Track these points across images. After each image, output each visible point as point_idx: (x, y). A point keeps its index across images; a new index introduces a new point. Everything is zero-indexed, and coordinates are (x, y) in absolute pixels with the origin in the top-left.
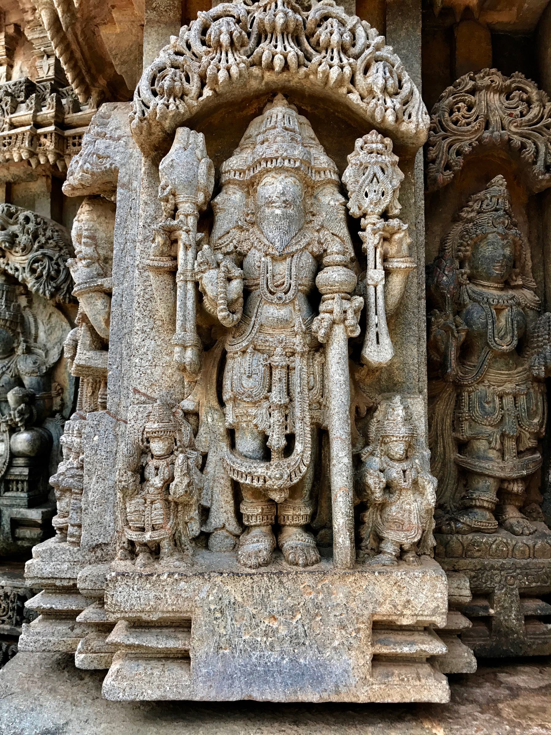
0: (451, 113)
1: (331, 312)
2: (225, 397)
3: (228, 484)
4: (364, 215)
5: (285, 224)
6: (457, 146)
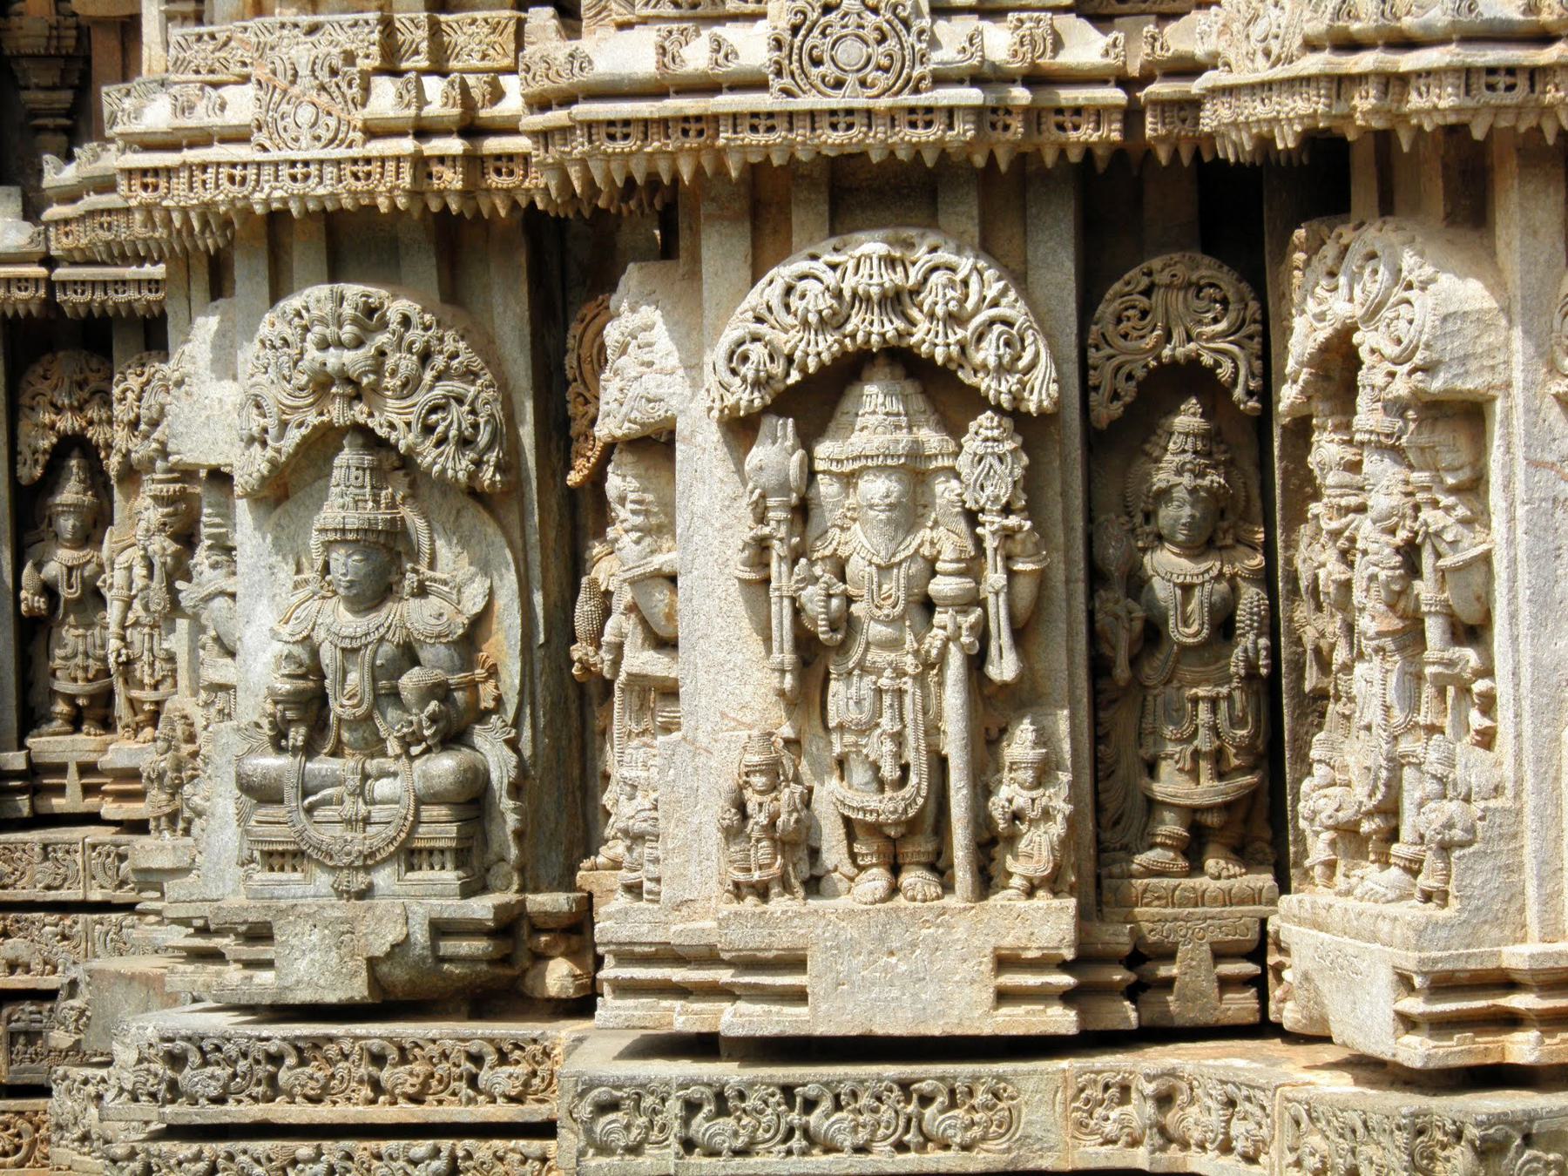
0: (1119, 321)
1: (944, 628)
2: (832, 724)
3: (840, 821)
4: (982, 510)
5: (890, 530)
6: (1125, 370)
